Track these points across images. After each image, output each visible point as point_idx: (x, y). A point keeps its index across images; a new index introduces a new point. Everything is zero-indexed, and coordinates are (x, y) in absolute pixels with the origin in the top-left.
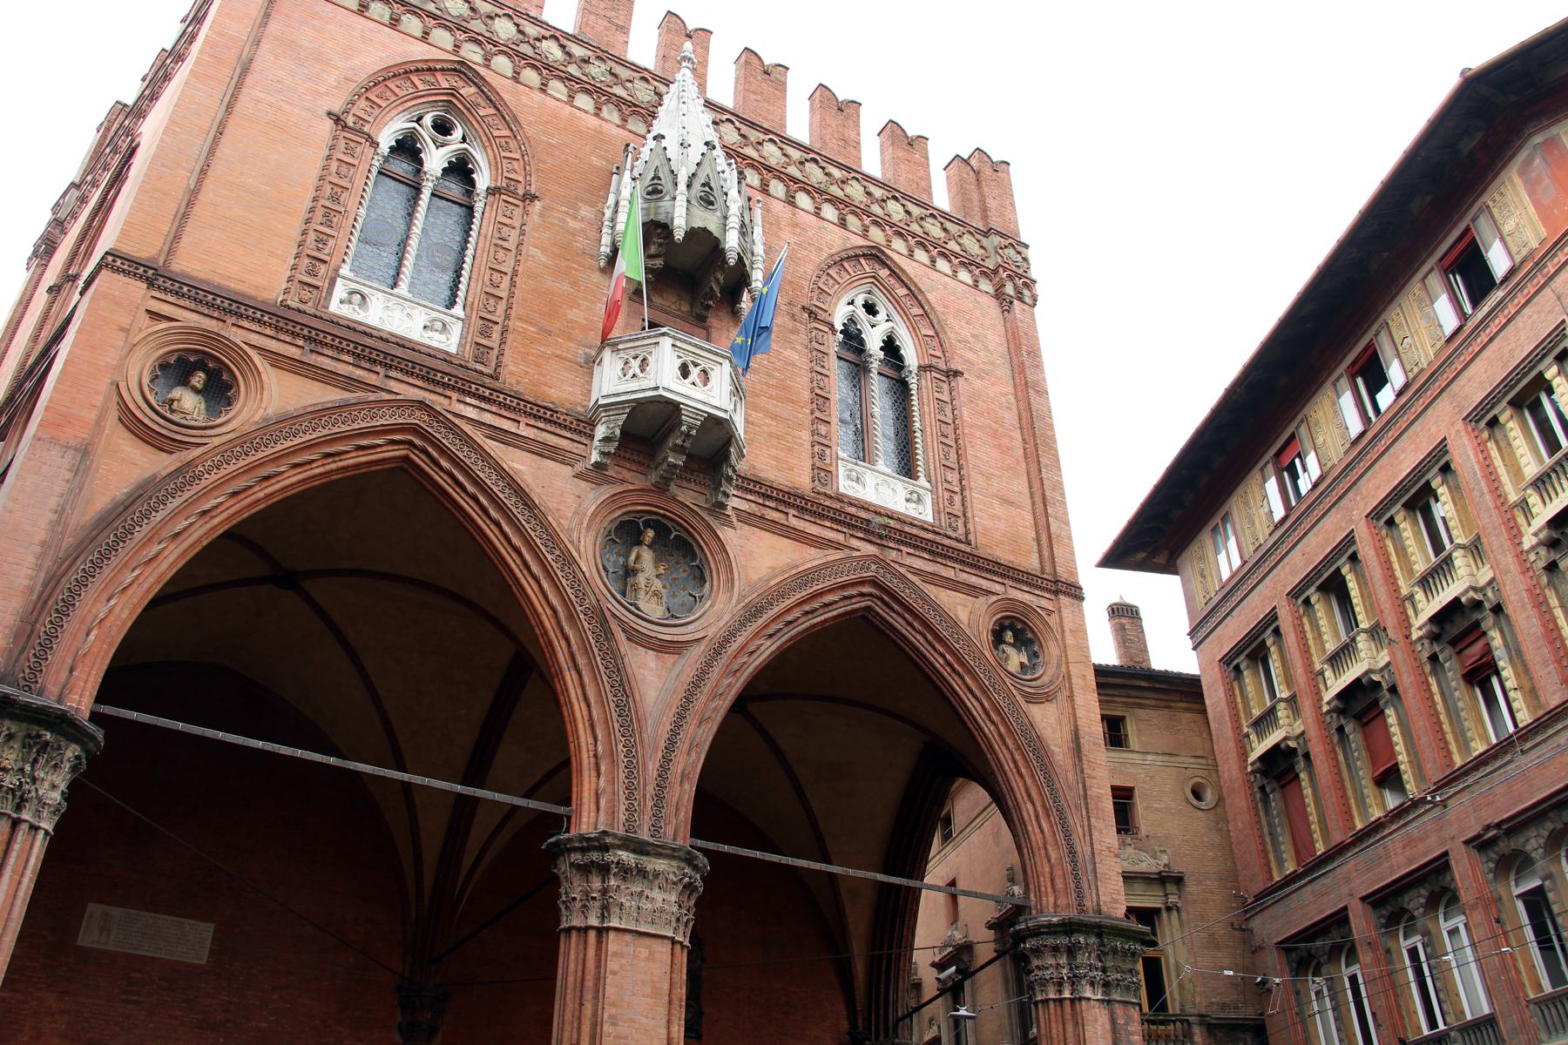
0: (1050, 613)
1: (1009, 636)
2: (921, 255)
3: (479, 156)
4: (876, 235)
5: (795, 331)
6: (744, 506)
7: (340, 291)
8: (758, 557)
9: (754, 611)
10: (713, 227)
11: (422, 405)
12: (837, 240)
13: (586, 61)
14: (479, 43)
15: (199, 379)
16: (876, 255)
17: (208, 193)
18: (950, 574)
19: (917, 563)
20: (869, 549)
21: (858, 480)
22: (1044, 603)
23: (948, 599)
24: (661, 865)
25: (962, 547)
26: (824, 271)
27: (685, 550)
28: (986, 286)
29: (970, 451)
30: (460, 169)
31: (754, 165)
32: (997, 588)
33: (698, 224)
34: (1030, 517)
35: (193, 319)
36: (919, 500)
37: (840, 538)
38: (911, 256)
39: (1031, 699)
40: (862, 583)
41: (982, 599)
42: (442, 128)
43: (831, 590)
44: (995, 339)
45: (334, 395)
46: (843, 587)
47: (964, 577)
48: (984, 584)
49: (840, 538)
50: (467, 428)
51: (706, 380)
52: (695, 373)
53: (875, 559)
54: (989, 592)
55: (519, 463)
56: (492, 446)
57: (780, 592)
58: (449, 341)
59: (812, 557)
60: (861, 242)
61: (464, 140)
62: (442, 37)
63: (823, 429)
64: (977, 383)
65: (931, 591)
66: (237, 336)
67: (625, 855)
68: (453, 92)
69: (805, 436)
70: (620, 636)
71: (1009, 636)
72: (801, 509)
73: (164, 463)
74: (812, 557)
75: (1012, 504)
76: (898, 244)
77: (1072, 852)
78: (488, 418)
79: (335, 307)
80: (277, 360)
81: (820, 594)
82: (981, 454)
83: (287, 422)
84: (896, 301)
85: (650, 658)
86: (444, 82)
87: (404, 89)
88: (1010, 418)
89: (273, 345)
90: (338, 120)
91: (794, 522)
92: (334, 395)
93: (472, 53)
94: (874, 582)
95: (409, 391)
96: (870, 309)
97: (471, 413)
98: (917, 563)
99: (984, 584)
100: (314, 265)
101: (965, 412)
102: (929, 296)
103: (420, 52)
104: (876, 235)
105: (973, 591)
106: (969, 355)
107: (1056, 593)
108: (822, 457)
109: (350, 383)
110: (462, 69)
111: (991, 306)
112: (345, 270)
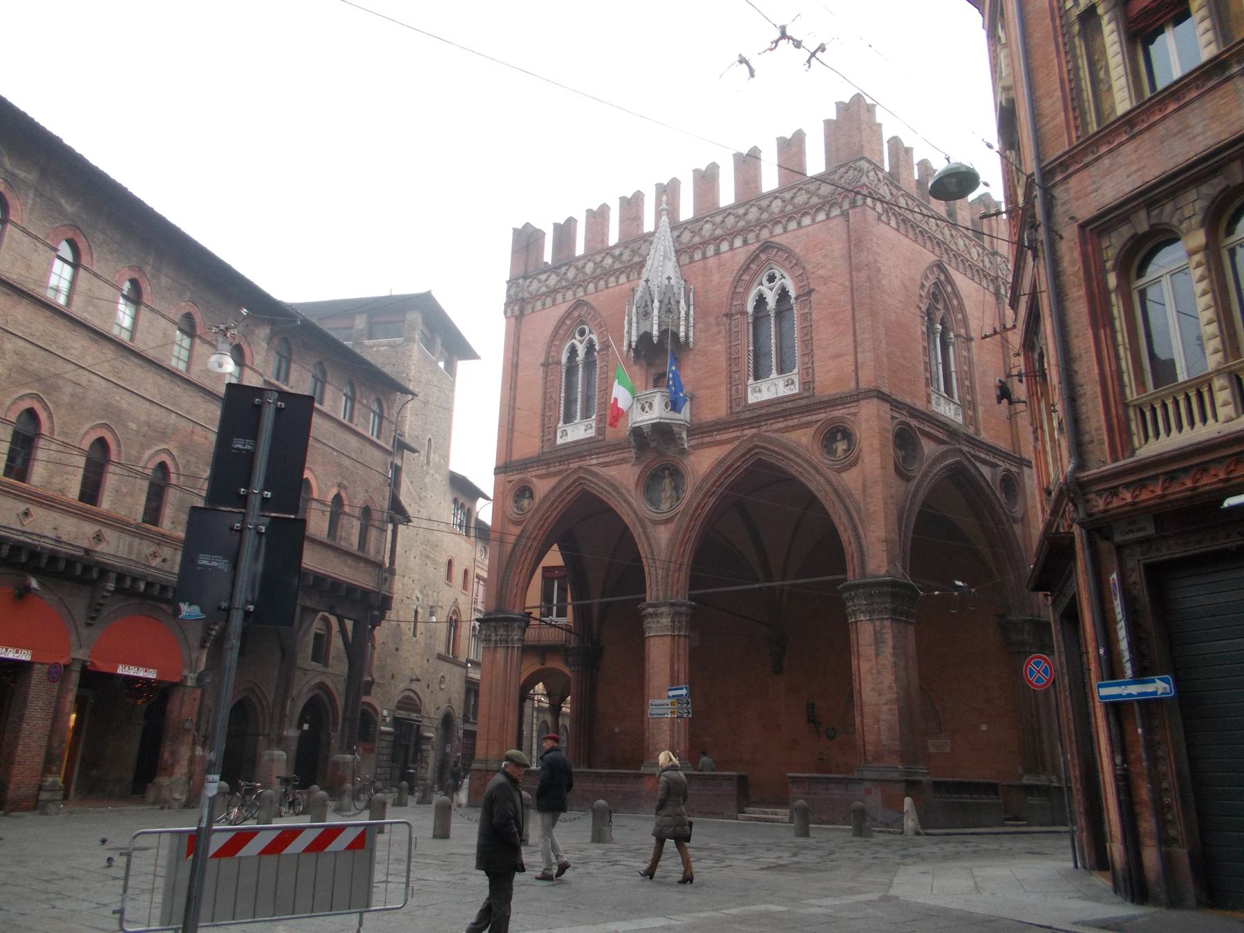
0: (855, 414)
1: (839, 436)
2: (792, 225)
3: (594, 337)
4: (765, 234)
5: (719, 332)
6: (694, 442)
7: (559, 434)
8: (703, 462)
9: (698, 489)
10: (648, 329)
11: (580, 468)
12: (741, 256)
13: (621, 255)
14: (580, 286)
15: (527, 494)
16: (766, 247)
17: (516, 426)
18: (796, 422)
19: (776, 426)
20: (755, 430)
21: (760, 391)
22: (853, 410)
23: (793, 436)
24: (663, 609)
25: (804, 402)
26: (738, 280)
27: (676, 473)
28: (835, 212)
29: (815, 338)
30: (590, 347)
31: (695, 247)
32: (823, 415)
33: (642, 332)
34: (851, 358)
35: (516, 477)
36: (793, 383)
37: (739, 433)
38: (785, 230)
39: (839, 471)
40: (752, 449)
41: (815, 427)
42: (582, 333)
43: (736, 461)
44: (838, 247)
45: (557, 479)
46: (743, 455)
47: (804, 419)
48: (814, 418)
49: (739, 433)
50: (593, 469)
51: (651, 406)
52: (647, 406)
53: (754, 436)
54: (817, 421)
55: (612, 472)
56: (604, 471)
57: (711, 473)
58: (591, 433)
59: (728, 448)
60: (757, 245)
61: (590, 332)
62: (569, 294)
63: (737, 376)
64: (822, 289)
65: (787, 435)
66: (528, 476)
67: (650, 610)
68: (579, 316)
69: (723, 389)
70: (649, 524)
71: (839, 436)
72: (718, 430)
73: (520, 528)
74: (728, 448)
75: (839, 356)
76: (779, 229)
77: (860, 546)
78: (601, 460)
79: (559, 441)
80: (540, 477)
81: (732, 465)
82: (824, 334)
83: (546, 497)
84: (783, 266)
85: (662, 528)
86: (576, 314)
87: (565, 327)
88: (844, 298)
89: (538, 473)
90: (543, 365)
91: (718, 438)
92: (557, 479)
93: (580, 293)
94: (756, 446)
95: (574, 466)
96: (772, 279)
97: (595, 462)
98: (776, 426)
99: (814, 418)
100: (548, 431)
101: (814, 317)
102: (797, 251)
103: (563, 308)
104: (765, 234)
105: (808, 425)
106: (822, 272)
107: (858, 401)
108: (737, 391)
109: (559, 473)
110: (579, 303)
111: (838, 224)
112: (561, 424)
